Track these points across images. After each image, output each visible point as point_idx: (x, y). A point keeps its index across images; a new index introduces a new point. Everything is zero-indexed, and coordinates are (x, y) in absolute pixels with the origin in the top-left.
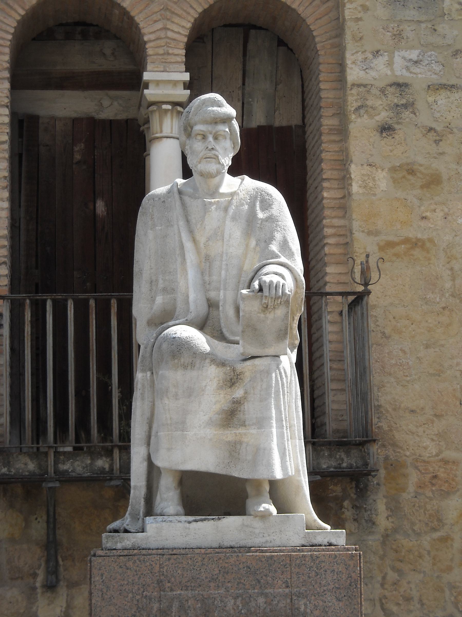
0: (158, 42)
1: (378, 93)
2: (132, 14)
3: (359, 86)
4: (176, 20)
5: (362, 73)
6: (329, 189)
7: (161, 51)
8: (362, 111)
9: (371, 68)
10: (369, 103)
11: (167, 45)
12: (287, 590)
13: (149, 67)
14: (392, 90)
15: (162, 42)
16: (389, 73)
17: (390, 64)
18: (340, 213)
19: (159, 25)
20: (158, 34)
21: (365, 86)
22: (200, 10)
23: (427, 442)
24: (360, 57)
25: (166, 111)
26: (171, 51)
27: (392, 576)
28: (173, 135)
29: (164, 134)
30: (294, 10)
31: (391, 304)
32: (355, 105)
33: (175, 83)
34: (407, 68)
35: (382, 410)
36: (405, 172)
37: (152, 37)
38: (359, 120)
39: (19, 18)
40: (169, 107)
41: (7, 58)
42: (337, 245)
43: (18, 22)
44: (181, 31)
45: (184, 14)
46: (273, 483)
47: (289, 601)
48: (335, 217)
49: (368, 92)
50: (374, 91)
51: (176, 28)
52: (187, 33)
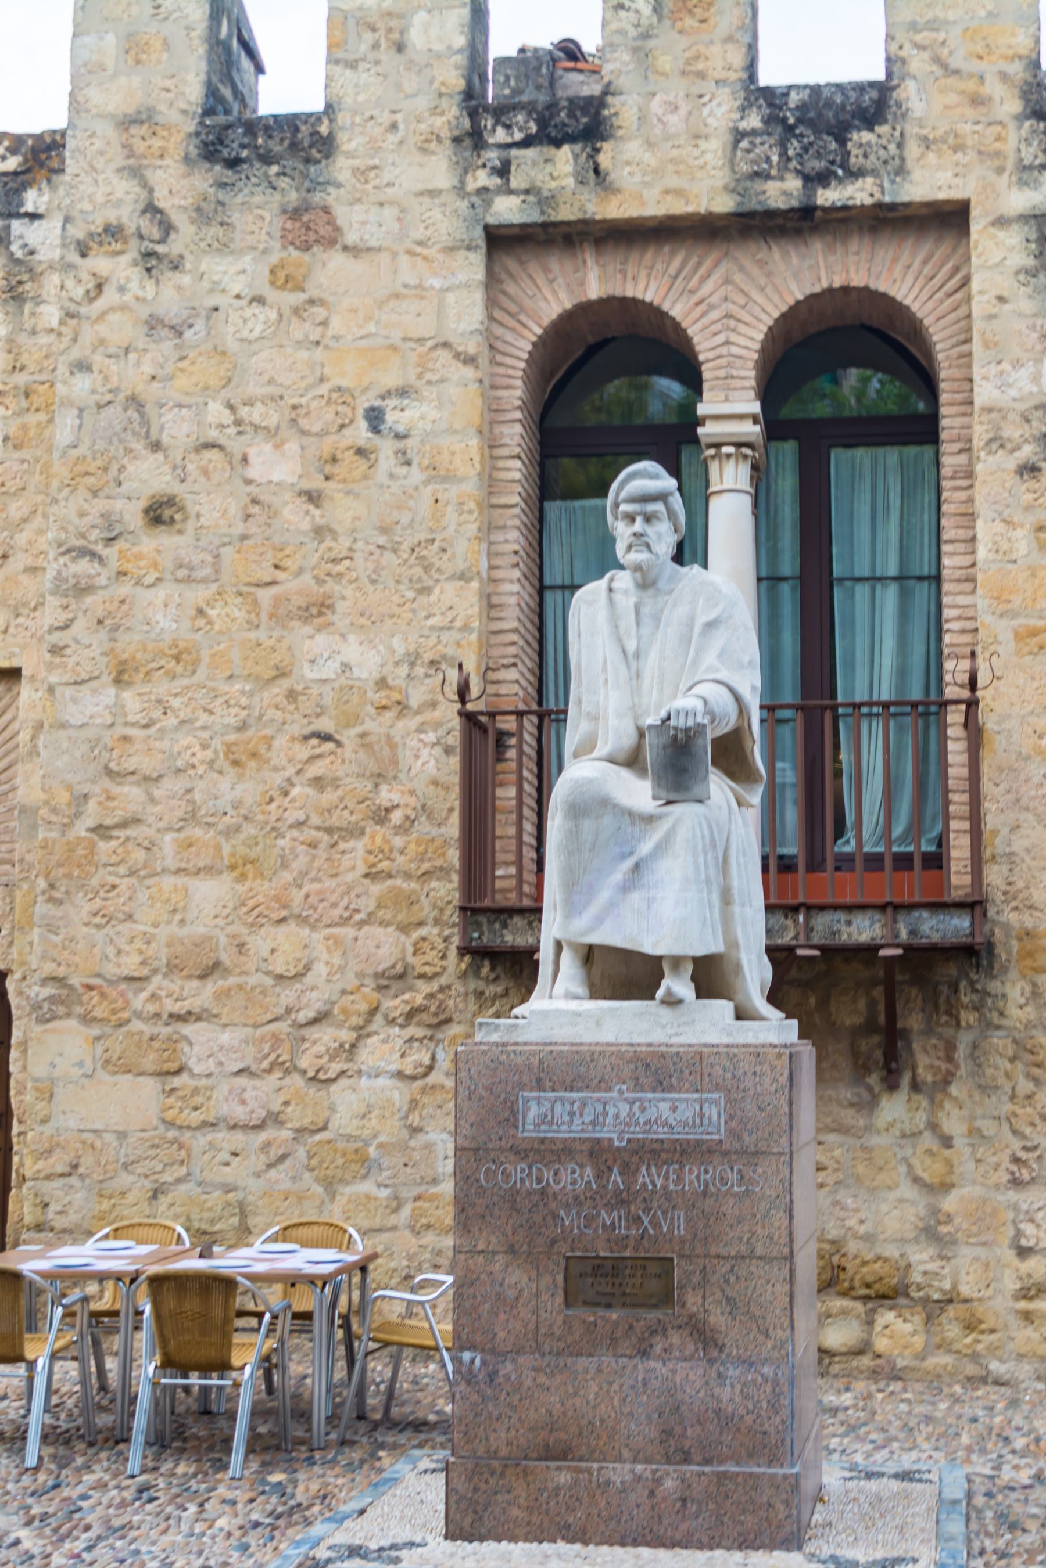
0: (719, 361)
1: (1018, 419)
2: (684, 325)
3: (990, 410)
4: (742, 328)
5: (996, 393)
6: (953, 554)
7: (722, 373)
8: (994, 446)
9: (1010, 386)
10: (1005, 434)
11: (729, 365)
12: (696, 1096)
13: (706, 395)
15: (723, 362)
16: (1035, 389)
19: (721, 338)
20: (718, 352)
21: (1000, 410)
22: (776, 314)
24: (993, 369)
25: (729, 456)
26: (735, 373)
27: (1025, 1086)
28: (739, 487)
29: (725, 486)
30: (908, 308)
31: (1032, 713)
32: (986, 437)
33: (741, 417)
35: (1017, 860)
37: (711, 355)
38: (991, 459)
39: (534, 339)
40: (731, 449)
43: (534, 344)
44: (750, 344)
45: (755, 322)
48: (960, 593)
49: (1004, 418)
50: (1011, 416)
51: (742, 341)
52: (757, 346)
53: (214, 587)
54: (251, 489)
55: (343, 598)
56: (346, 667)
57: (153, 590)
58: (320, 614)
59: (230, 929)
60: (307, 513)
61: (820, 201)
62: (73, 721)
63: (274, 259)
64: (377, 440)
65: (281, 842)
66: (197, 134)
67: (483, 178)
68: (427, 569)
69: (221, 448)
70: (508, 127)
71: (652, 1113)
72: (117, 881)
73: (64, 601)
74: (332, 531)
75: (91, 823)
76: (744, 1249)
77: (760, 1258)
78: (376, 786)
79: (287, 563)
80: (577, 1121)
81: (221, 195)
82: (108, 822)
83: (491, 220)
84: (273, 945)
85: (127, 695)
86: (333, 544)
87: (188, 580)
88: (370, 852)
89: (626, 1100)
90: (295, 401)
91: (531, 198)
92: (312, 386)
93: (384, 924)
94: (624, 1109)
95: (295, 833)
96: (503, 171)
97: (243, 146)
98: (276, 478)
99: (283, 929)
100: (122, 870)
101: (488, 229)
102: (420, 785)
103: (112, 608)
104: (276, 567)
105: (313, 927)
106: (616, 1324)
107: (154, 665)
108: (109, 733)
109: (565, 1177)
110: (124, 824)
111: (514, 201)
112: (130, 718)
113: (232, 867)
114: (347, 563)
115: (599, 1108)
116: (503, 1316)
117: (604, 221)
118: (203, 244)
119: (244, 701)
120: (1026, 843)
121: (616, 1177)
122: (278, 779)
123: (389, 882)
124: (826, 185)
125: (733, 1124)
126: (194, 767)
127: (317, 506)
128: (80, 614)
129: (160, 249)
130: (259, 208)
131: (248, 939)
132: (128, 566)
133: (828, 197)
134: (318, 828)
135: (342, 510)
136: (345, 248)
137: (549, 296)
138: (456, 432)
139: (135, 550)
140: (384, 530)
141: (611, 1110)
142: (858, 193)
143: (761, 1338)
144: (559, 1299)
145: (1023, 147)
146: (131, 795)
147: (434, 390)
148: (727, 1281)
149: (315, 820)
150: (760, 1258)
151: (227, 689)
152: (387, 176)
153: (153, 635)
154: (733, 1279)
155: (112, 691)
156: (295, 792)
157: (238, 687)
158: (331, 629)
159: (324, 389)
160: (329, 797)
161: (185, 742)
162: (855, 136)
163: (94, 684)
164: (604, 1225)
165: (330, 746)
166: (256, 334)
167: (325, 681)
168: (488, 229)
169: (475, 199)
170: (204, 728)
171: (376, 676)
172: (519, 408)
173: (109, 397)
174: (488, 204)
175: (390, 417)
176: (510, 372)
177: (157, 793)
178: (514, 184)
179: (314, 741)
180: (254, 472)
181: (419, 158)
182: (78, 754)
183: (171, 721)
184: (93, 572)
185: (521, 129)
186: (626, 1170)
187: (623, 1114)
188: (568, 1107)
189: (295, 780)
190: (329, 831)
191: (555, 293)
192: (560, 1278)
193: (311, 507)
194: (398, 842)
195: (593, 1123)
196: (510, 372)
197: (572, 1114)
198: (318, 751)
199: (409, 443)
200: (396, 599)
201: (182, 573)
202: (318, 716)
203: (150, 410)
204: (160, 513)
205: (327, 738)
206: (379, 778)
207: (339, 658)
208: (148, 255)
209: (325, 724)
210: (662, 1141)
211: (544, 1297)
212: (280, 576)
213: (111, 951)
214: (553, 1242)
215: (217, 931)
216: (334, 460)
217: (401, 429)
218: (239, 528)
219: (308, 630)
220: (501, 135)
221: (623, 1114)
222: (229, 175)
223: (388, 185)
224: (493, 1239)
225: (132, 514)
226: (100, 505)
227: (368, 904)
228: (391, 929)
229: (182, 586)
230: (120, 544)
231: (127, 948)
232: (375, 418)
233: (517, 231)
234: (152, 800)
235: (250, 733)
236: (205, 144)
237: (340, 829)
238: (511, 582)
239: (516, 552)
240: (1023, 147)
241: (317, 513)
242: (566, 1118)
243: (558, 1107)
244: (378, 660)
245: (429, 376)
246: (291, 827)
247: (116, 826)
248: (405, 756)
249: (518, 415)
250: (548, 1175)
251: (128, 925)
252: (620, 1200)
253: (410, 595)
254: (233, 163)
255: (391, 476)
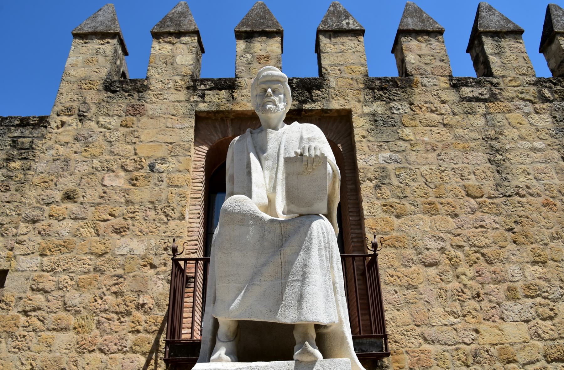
6: (352, 216)
14: (379, 170)
17: (377, 158)
18: (359, 227)
23: (413, 340)
24: (363, 157)
34: (385, 161)
36: (388, 207)
41: (204, 163)
42: (358, 242)
46: (318, 327)
48: (356, 229)
50: (370, 170)
53: (85, 221)
54: (104, 188)
55: (134, 225)
56: (131, 251)
57: (61, 222)
58: (125, 231)
59: (70, 355)
60: (124, 196)
61: (304, 108)
62: (21, 269)
63: (123, 118)
64: (152, 174)
65: (96, 318)
66: (103, 83)
67: (196, 98)
68: (167, 216)
69: (96, 175)
70: (205, 85)
72: (26, 333)
73: (27, 225)
74: (132, 202)
75: (20, 309)
78: (139, 295)
79: (114, 213)
81: (109, 100)
82: (28, 309)
83: (197, 109)
84: (88, 361)
85: (45, 259)
86: (132, 207)
87: (75, 219)
88: (133, 322)
90: (124, 160)
91: (211, 104)
92: (131, 156)
93: (135, 352)
95: (103, 315)
96: (203, 96)
97: (118, 87)
98: (114, 185)
99: (93, 354)
100: (30, 329)
101: (196, 112)
102: (155, 295)
103: (44, 227)
104: (110, 215)
105: (105, 354)
107: (57, 249)
108: (34, 274)
110: (34, 310)
111: (206, 105)
112: (45, 268)
113: (75, 328)
114: (137, 213)
117: (234, 112)
118: (100, 113)
119: (90, 262)
120: (391, 317)
122: (98, 293)
123: (140, 335)
124: (306, 104)
126: (66, 287)
127: (128, 194)
128: (32, 229)
129: (85, 114)
130: (121, 103)
131: (78, 359)
132: (53, 213)
133: (307, 106)
134: (113, 312)
135: (136, 195)
136: (148, 116)
137: (215, 135)
138: (180, 171)
139: (57, 207)
140: (152, 203)
142: (316, 106)
145: (366, 97)
146: (39, 298)
147: (174, 158)
149: (112, 309)
151: (84, 257)
152: (165, 97)
153: (58, 238)
155: (39, 258)
156: (105, 298)
157: (89, 257)
158: (127, 237)
159: (135, 157)
160: (120, 300)
161: (63, 278)
162: (314, 91)
163: (32, 255)
165: (121, 280)
166: (114, 140)
167: (122, 255)
168: (196, 112)
169: (192, 104)
170: (73, 272)
171: (143, 253)
172: (203, 167)
173: (58, 157)
174: (197, 105)
175: (157, 166)
176: (201, 156)
177: (50, 297)
178: (206, 100)
179: (115, 278)
180: (105, 183)
181: (174, 92)
182: (20, 282)
183: (60, 269)
184: (40, 215)
185: (209, 85)
189: (106, 293)
190: (117, 313)
191: (217, 134)
193: (126, 194)
194: (144, 318)
196: (201, 156)
198: (117, 281)
199: (164, 174)
200: (154, 226)
201: (72, 216)
202: (118, 268)
203: (72, 163)
204: (69, 197)
205: (121, 277)
206: (139, 292)
207: (129, 247)
208: (80, 115)
209: (120, 272)
212: (110, 218)
213: (18, 363)
215: (64, 355)
216: (137, 179)
217: (162, 170)
218: (98, 200)
219: (118, 236)
220: (203, 87)
222: (112, 95)
223: (165, 99)
225: (58, 195)
226: (48, 192)
227: (129, 344)
228: (138, 355)
229: (72, 221)
230: (52, 206)
231: (24, 362)
232: (152, 167)
233: (205, 115)
234: (48, 301)
235: (91, 274)
236: (106, 86)
237: (121, 313)
238: (197, 223)
239: (199, 214)
240: (366, 97)
241: (127, 196)
244: (144, 248)
245: (173, 154)
246: (101, 312)
247: (31, 311)
248: (151, 285)
249: (203, 169)
251: (28, 352)
253: (159, 225)
254: (114, 92)
255: (156, 185)
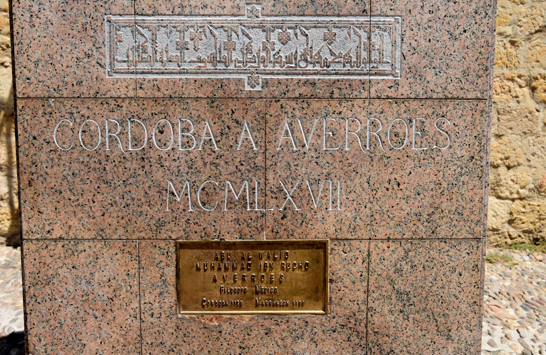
12: (362, 19)
47: (364, 35)
71: (297, 45)
76: (423, 230)
77: (444, 240)
80: (190, 56)
89: (262, 27)
94: (258, 38)
106: (248, 329)
109: (175, 138)
115: (221, 37)
116: (91, 321)
121: (246, 135)
125: (413, 60)
141: (240, 42)
143: (441, 340)
144: (171, 299)
148: (398, 271)
150: (444, 240)
154: (406, 268)
164: (231, 201)
186: (262, 123)
187: (256, 46)
188: (176, 37)
192: (170, 272)
195: (214, 60)
197: (182, 47)
210: (313, 84)
211: (148, 297)
214: (160, 224)
221: (256, 46)
224: (74, 222)
242: (174, 53)
243: (161, 35)
250: (149, 133)
252: (256, 166)
